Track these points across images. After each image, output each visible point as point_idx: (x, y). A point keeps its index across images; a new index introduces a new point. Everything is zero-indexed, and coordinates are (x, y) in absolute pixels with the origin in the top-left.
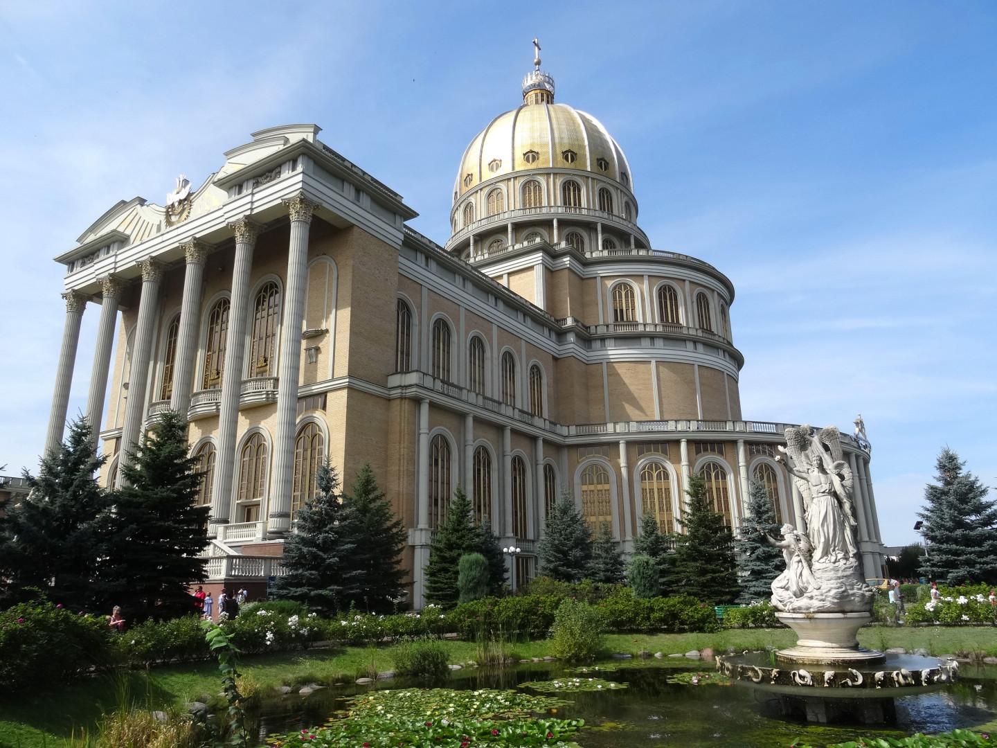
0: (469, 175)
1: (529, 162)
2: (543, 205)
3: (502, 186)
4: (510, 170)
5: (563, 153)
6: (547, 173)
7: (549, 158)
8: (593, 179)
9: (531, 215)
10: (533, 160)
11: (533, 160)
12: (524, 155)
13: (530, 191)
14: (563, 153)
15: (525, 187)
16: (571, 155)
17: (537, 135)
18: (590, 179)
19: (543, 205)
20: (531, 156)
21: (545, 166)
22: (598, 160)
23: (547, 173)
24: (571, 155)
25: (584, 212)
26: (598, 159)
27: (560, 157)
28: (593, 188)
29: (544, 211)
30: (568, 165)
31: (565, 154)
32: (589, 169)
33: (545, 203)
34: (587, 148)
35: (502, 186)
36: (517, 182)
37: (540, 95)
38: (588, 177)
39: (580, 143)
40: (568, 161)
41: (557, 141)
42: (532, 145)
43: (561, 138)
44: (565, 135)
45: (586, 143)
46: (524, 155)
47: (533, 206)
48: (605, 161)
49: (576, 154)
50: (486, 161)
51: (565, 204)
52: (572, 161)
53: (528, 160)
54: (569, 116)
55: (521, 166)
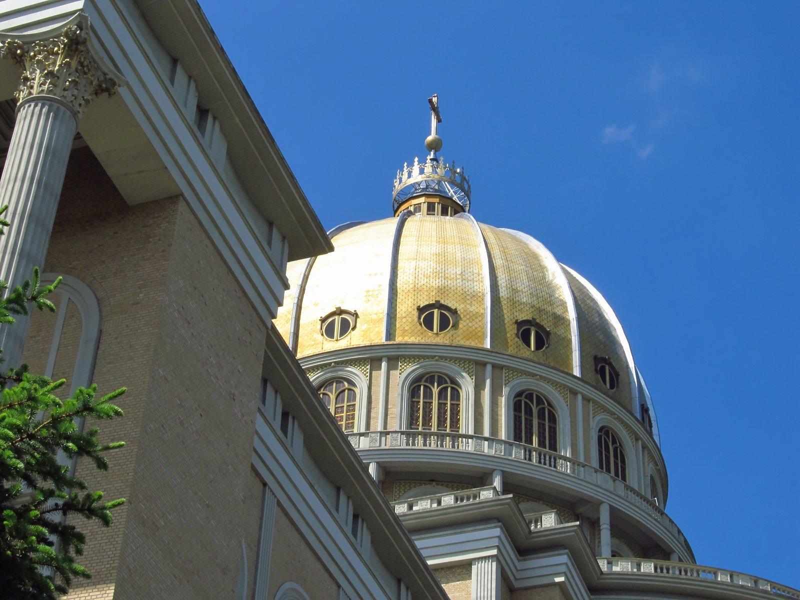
1: (431, 329)
2: (462, 431)
3: (359, 375)
4: (379, 337)
6: (477, 364)
7: (483, 328)
8: (586, 399)
9: (430, 448)
10: (444, 324)
11: (444, 324)
12: (421, 310)
13: (428, 394)
15: (416, 387)
17: (454, 271)
18: (580, 397)
19: (462, 431)
20: (437, 314)
21: (473, 343)
23: (477, 364)
25: (566, 468)
26: (597, 359)
27: (511, 331)
28: (586, 420)
29: (469, 446)
31: (524, 329)
32: (577, 372)
33: (467, 424)
35: (359, 375)
36: (394, 373)
38: (574, 393)
39: (559, 311)
41: (503, 293)
42: (442, 290)
44: (523, 284)
46: (421, 310)
47: (434, 429)
48: (611, 365)
49: (548, 334)
51: (517, 437)
52: (539, 346)
53: (428, 323)
55: (409, 333)
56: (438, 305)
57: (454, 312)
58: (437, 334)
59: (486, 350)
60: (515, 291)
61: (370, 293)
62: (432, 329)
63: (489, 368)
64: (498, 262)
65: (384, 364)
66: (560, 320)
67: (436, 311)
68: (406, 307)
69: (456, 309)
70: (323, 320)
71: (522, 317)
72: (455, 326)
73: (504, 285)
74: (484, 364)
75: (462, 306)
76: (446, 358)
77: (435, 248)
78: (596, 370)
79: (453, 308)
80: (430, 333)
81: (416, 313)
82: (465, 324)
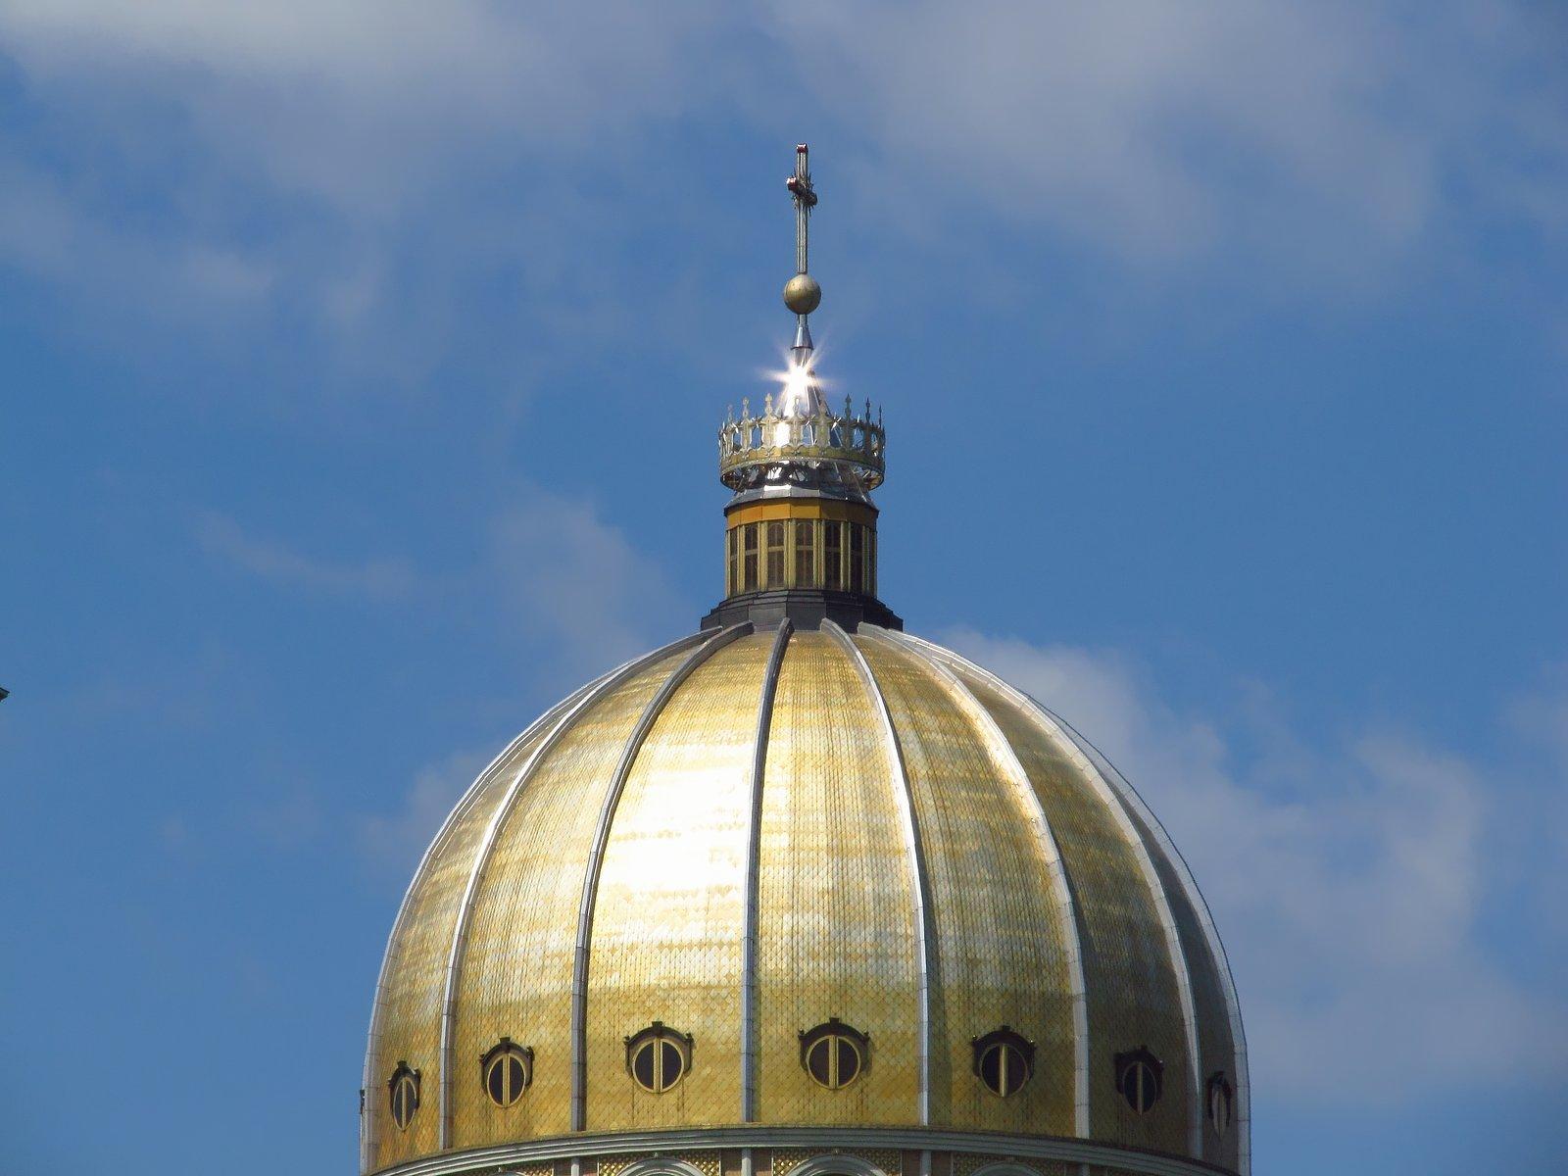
0: (506, 1045)
4: (736, 1116)
5: (978, 1045)
11: (845, 1075)
12: (805, 1039)
14: (978, 1045)
16: (1010, 1053)
17: (863, 938)
20: (835, 1049)
22: (1120, 1060)
24: (1007, 1055)
26: (1120, 1060)
27: (962, 1060)
30: (995, 1111)
31: (985, 1053)
32: (1082, 1128)
34: (1080, 1011)
37: (818, 533)
39: (1050, 985)
40: (995, 1086)
41: (951, 977)
42: (842, 989)
43: (971, 964)
44: (986, 950)
45: (1076, 984)
46: (805, 1039)
48: (1151, 1061)
50: (612, 1027)
53: (818, 1070)
54: (996, 820)
55: (790, 1104)
56: (835, 1026)
57: (864, 1040)
58: (835, 1090)
59: (923, 1130)
60: (971, 964)
61: (713, 992)
62: (826, 1082)
63: (926, 1161)
64: (943, 892)
65: (745, 1162)
66: (1055, 1005)
67: (831, 1038)
68: (780, 1033)
69: (867, 1034)
70: (631, 1043)
71: (985, 1026)
72: (867, 1066)
73: (952, 954)
74: (919, 1153)
75: (878, 1021)
76: (852, 1150)
77: (823, 881)
78: (1119, 1087)
79: (861, 1030)
80: (823, 1090)
81: (796, 1044)
82: (883, 1062)
